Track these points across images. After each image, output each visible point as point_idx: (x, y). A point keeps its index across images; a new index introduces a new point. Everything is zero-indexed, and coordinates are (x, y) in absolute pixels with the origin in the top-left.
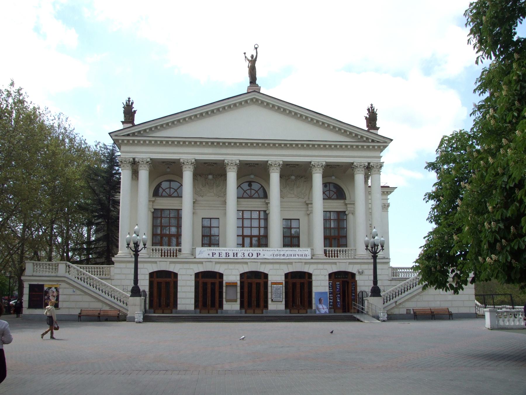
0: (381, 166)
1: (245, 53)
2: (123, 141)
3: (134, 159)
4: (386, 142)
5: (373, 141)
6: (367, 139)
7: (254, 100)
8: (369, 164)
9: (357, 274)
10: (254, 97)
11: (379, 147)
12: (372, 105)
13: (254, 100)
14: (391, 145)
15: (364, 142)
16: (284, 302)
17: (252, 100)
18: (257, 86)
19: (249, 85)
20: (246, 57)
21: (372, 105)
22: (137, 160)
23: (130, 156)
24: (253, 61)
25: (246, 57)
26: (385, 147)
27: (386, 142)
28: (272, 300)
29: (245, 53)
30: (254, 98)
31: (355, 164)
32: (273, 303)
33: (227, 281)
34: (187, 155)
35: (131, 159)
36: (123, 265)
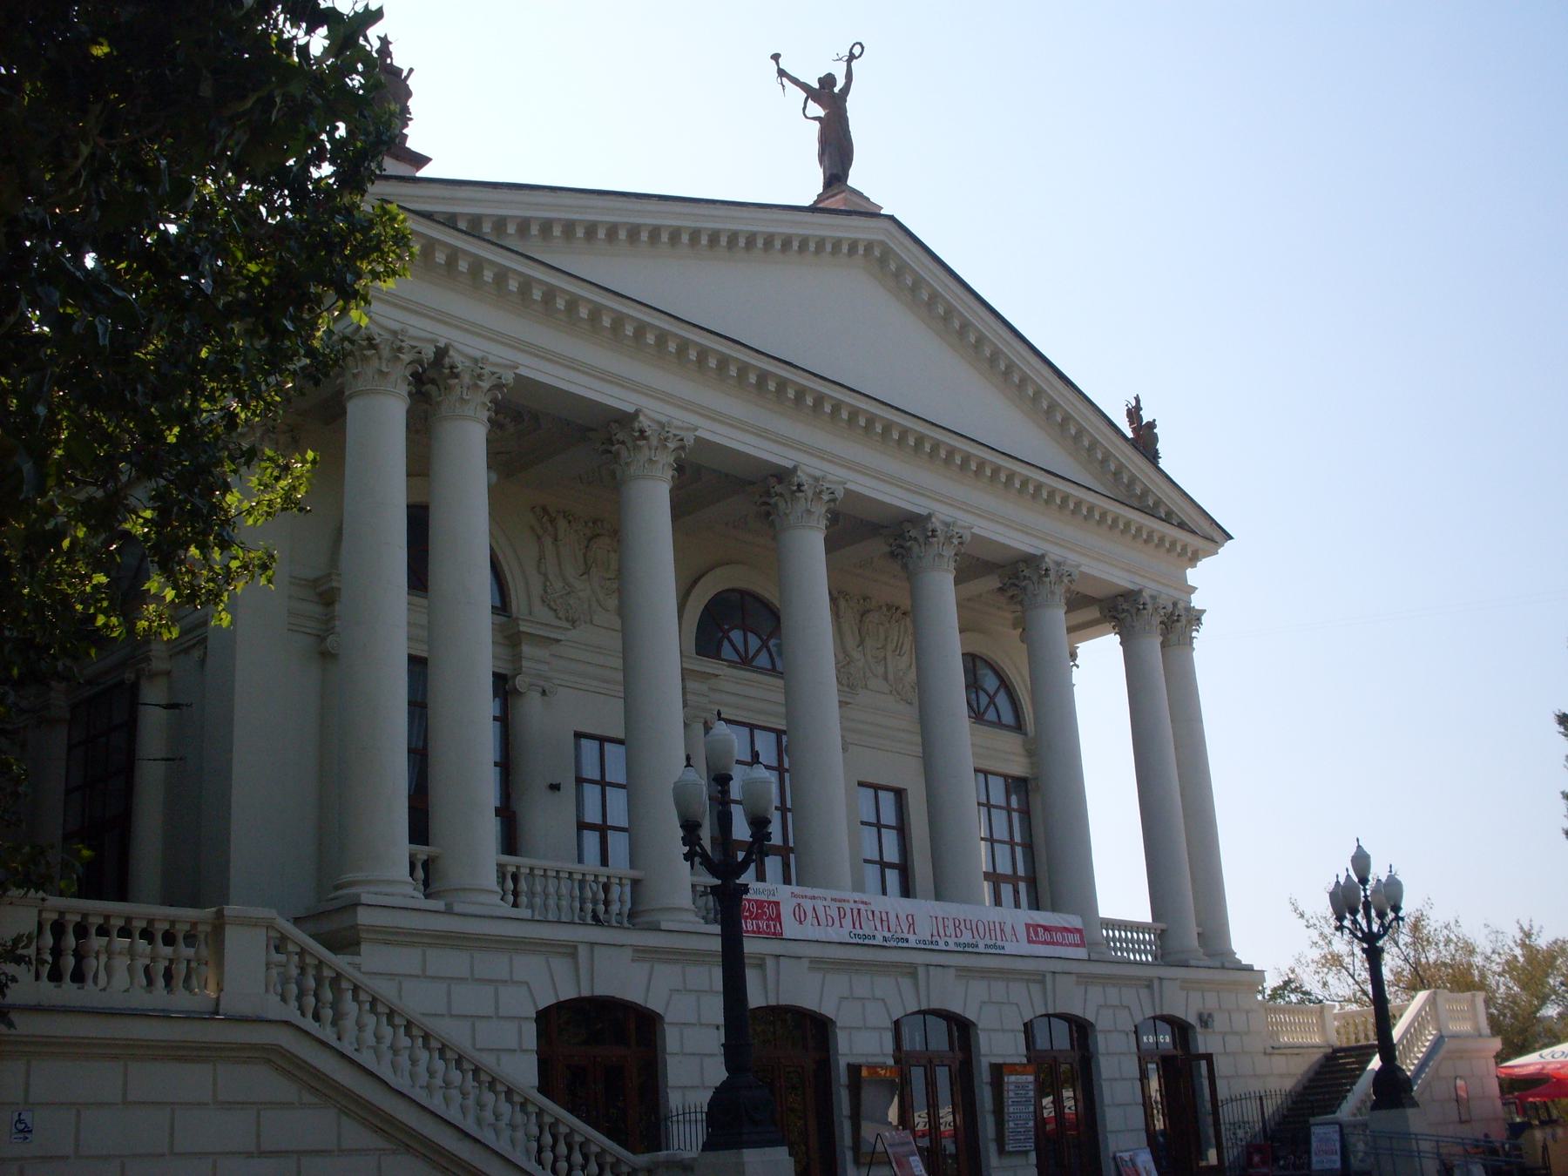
0: (1195, 618)
1: (776, 57)
3: (441, 353)
4: (1213, 540)
5: (1182, 525)
7: (877, 253)
9: (1198, 1029)
12: (1137, 399)
13: (877, 253)
14: (1227, 548)
16: (1033, 1157)
17: (869, 247)
20: (782, 73)
21: (1137, 399)
22: (455, 357)
23: (424, 332)
24: (830, 98)
25: (782, 73)
27: (1213, 540)
28: (1001, 1151)
29: (776, 57)
30: (882, 243)
31: (1146, 594)
32: (1006, 1161)
33: (853, 1060)
34: (680, 407)
35: (429, 352)
36: (404, 960)
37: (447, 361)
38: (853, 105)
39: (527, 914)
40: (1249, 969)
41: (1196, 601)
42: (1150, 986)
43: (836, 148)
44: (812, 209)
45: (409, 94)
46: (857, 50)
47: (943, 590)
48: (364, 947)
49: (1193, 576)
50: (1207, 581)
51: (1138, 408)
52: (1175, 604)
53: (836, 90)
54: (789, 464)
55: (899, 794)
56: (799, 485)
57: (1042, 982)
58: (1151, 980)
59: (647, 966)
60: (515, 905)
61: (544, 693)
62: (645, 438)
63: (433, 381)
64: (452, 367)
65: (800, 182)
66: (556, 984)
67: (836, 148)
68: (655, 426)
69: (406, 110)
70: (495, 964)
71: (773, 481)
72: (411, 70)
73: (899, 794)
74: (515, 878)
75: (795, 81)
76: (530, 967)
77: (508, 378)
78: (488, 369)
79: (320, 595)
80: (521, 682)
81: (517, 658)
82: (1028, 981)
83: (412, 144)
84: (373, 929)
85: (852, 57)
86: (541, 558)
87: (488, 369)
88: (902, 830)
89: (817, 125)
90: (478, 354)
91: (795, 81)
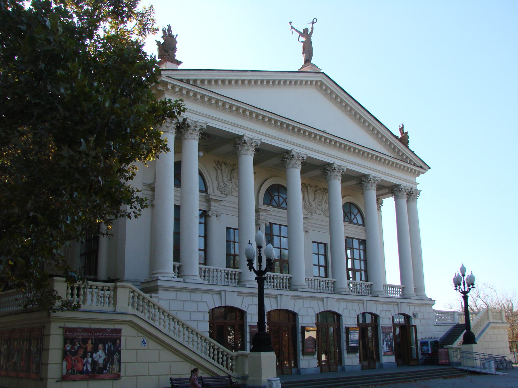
0: (418, 193)
1: (290, 23)
2: (174, 87)
5: (414, 165)
6: (411, 161)
7: (319, 84)
8: (411, 189)
9: (413, 317)
10: (311, 78)
11: (419, 172)
12: (403, 125)
13: (319, 84)
15: (407, 163)
17: (317, 82)
18: (314, 65)
19: (302, 63)
20: (292, 28)
21: (403, 125)
25: (292, 28)
26: (423, 173)
29: (290, 23)
30: (321, 81)
33: (303, 325)
36: (172, 295)
37: (186, 122)
38: (313, 38)
39: (207, 282)
40: (430, 300)
41: (419, 188)
42: (397, 305)
43: (308, 51)
44: (300, 72)
45: (176, 42)
46: (315, 21)
47: (337, 185)
48: (160, 292)
49: (418, 179)
50: (422, 182)
51: (403, 128)
52: (411, 189)
53: (308, 33)
54: (290, 149)
55: (325, 245)
56: (293, 155)
57: (363, 303)
58: (398, 303)
59: (242, 297)
60: (204, 280)
61: (217, 216)
62: (246, 143)
63: (183, 128)
64: (188, 124)
65: (296, 62)
66: (213, 302)
67: (308, 51)
68: (249, 139)
69: (175, 47)
70: (197, 296)
71: (285, 154)
72: (177, 35)
73: (325, 245)
74: (205, 272)
75: (296, 30)
76: (207, 297)
77: (205, 127)
78: (199, 124)
79: (151, 188)
80: (210, 213)
81: (209, 206)
82: (358, 303)
83: (178, 58)
84: (162, 287)
85: (313, 23)
86: (217, 176)
87: (199, 124)
88: (326, 255)
89: (302, 44)
90: (196, 120)
91: (296, 30)
